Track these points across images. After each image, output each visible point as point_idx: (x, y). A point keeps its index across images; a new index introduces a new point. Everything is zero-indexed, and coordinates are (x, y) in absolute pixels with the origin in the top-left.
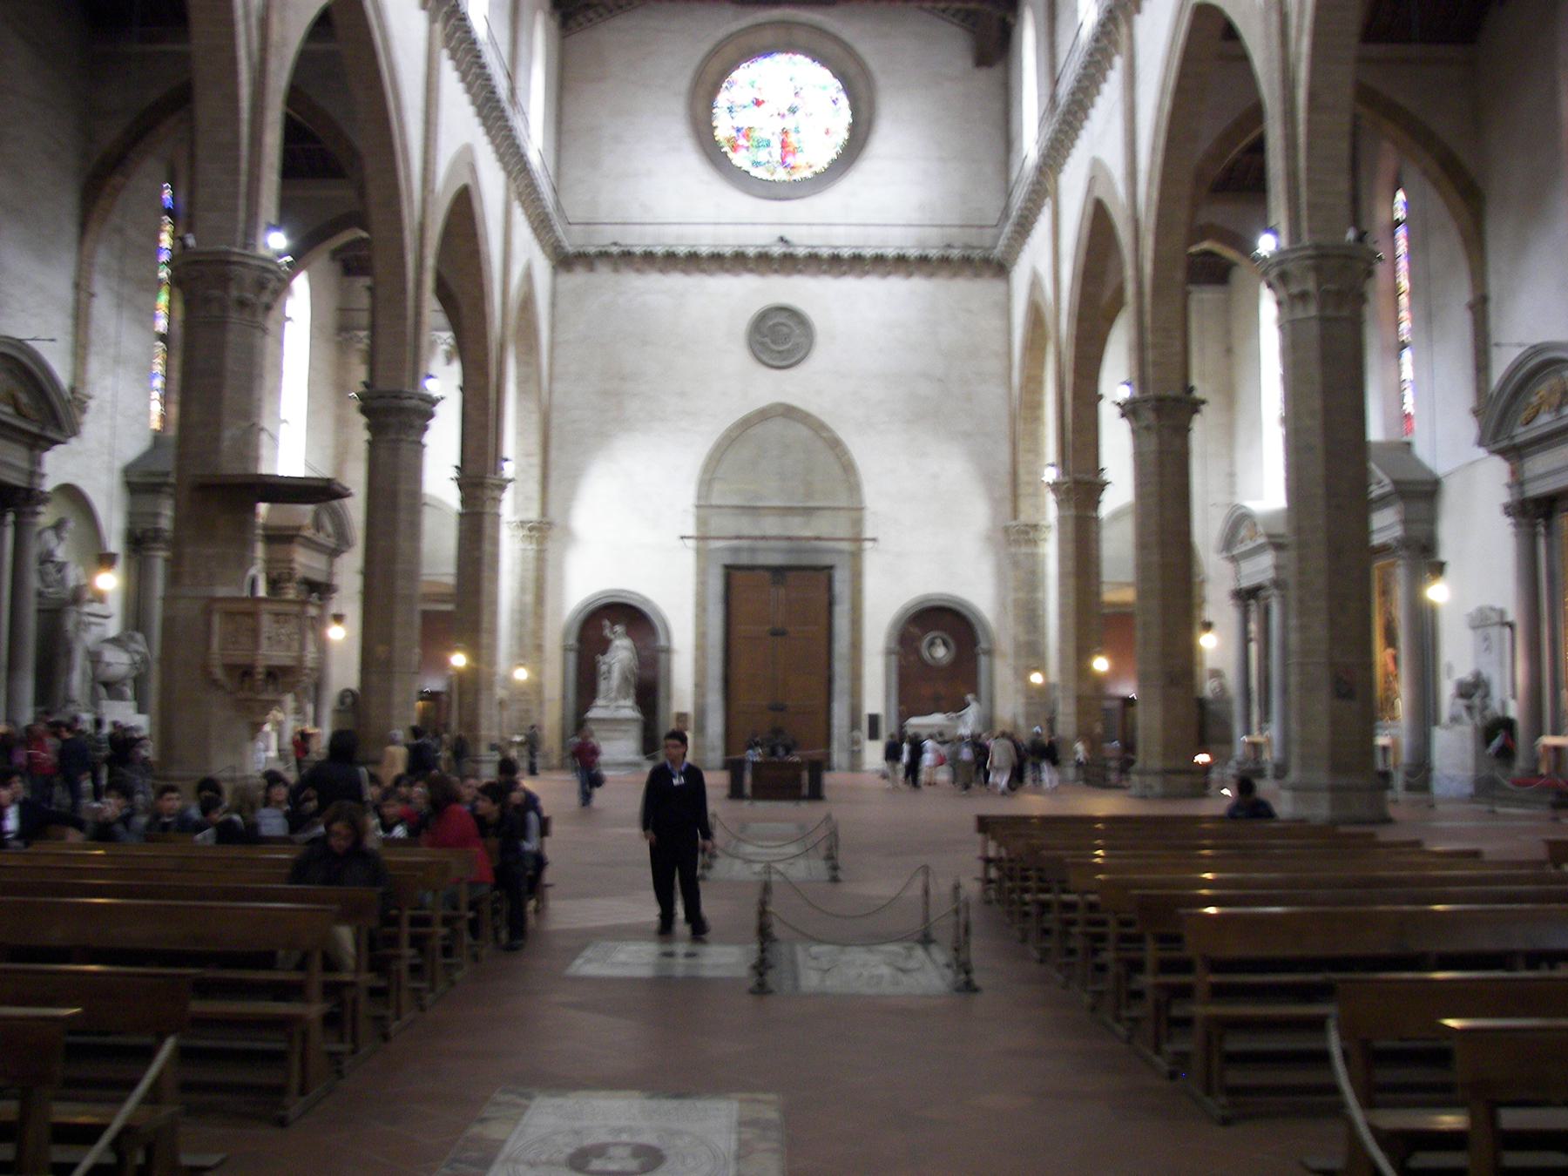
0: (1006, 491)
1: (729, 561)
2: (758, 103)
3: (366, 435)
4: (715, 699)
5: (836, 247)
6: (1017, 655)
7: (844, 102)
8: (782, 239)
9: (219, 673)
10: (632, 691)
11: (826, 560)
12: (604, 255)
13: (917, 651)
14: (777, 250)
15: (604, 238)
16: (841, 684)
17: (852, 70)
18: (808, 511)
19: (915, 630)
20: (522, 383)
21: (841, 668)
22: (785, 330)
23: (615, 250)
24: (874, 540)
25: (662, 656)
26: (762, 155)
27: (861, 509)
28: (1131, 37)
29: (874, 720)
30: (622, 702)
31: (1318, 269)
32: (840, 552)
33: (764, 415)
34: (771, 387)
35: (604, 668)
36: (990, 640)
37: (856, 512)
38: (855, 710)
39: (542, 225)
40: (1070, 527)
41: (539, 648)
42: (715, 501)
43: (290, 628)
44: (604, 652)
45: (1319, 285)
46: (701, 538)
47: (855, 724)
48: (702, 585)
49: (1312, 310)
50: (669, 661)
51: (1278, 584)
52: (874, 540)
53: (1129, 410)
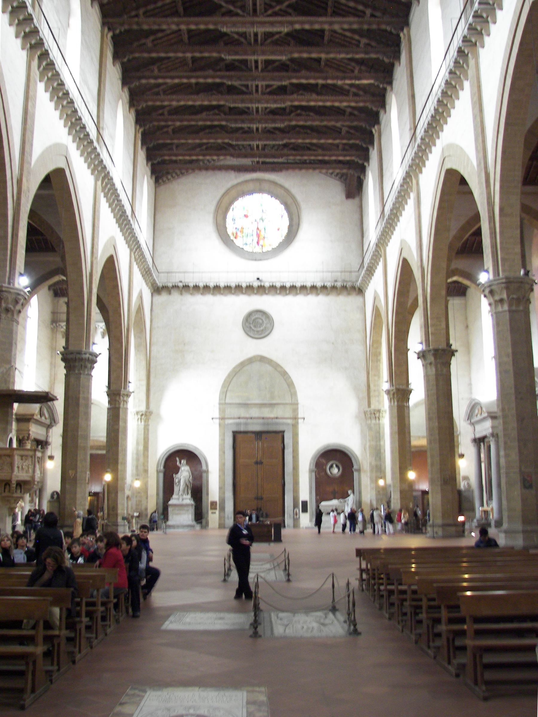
1: (235, 429)
3: (65, 371)
6: (371, 471)
7: (286, 215)
8: (258, 279)
10: (190, 492)
11: (281, 428)
12: (175, 287)
14: (256, 284)
15: (175, 279)
17: (290, 201)
18: (272, 405)
19: (324, 461)
20: (137, 347)
22: (260, 321)
23: (180, 285)
25: (204, 475)
27: (297, 404)
28: (418, 184)
29: (305, 504)
30: (184, 496)
31: (507, 288)
32: (288, 424)
33: (251, 361)
35: (176, 481)
37: (295, 406)
39: (146, 273)
40: (395, 411)
41: (146, 471)
42: (228, 401)
43: (29, 462)
44: (177, 472)
45: (508, 296)
46: (222, 418)
47: (295, 506)
49: (506, 307)
51: (492, 435)
53: (422, 355)
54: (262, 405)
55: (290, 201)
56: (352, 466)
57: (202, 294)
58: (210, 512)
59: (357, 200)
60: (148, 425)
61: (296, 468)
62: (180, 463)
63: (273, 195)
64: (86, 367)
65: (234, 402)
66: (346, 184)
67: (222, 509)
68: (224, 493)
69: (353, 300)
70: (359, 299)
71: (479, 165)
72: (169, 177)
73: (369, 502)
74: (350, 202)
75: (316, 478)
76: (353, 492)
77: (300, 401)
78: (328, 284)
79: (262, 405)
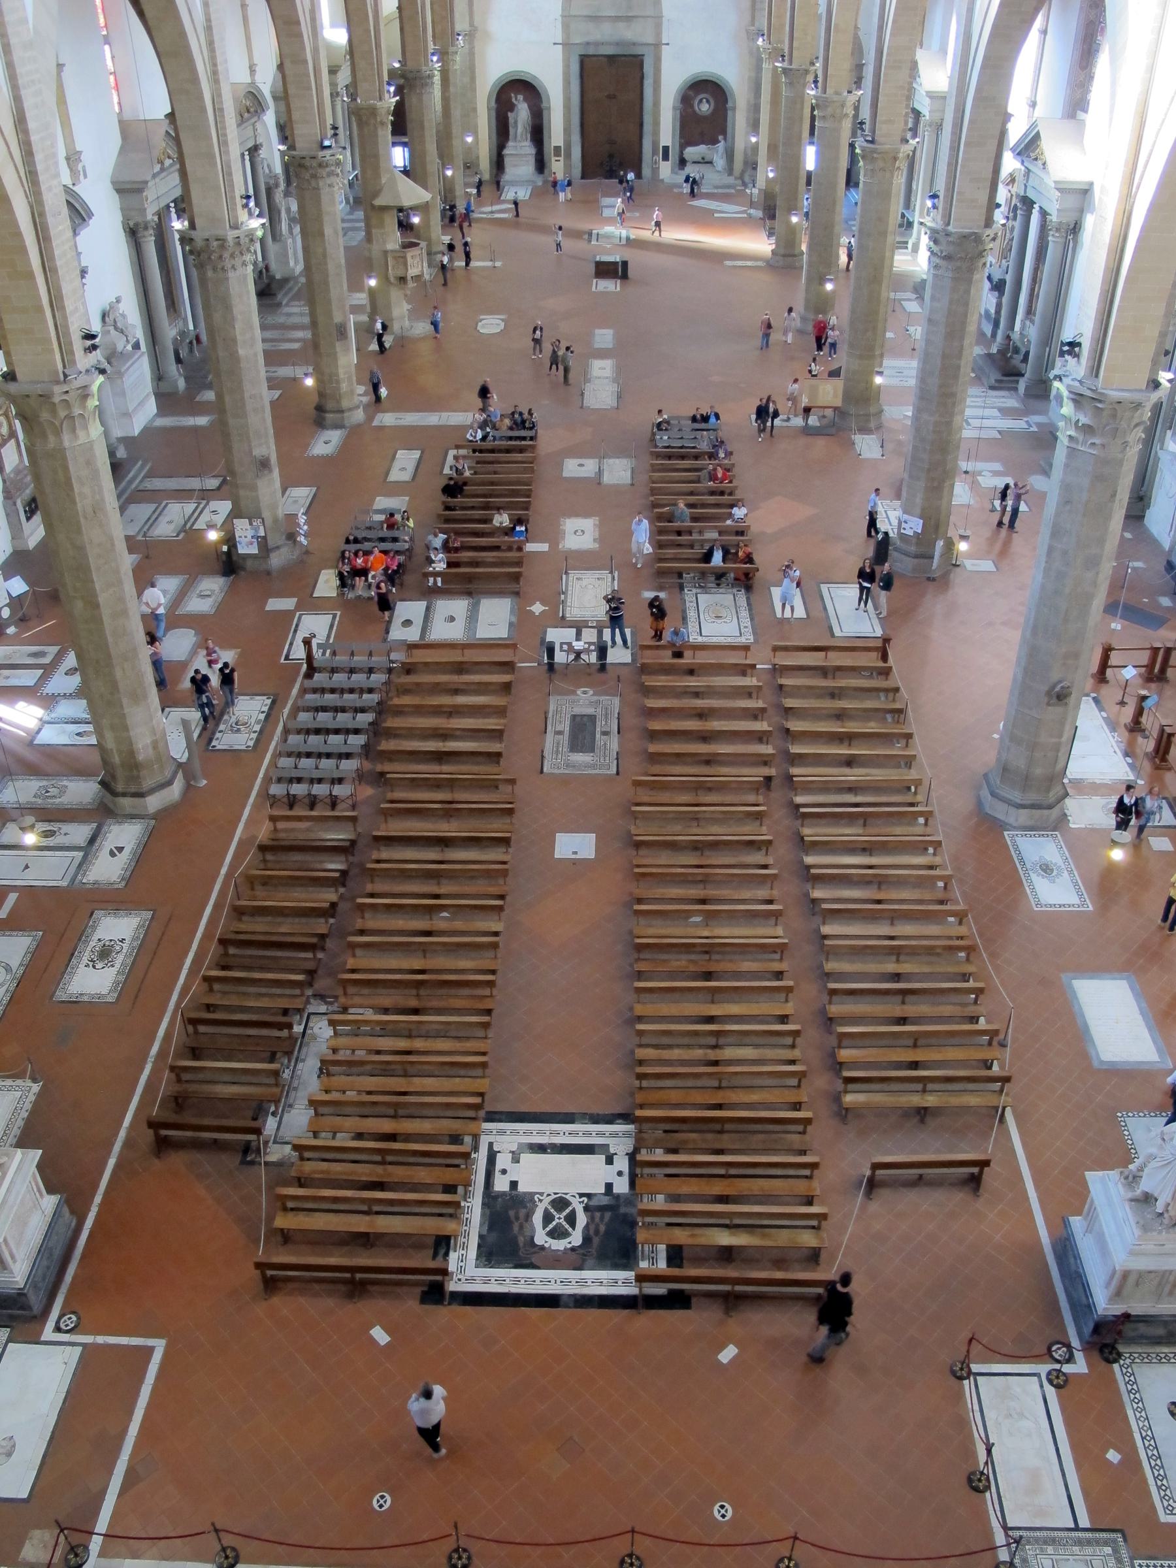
9: (392, 279)
13: (692, 106)
16: (648, 128)
18: (629, 19)
24: (668, 44)
27: (662, 17)
29: (666, 149)
35: (511, 121)
36: (735, 102)
37: (658, 20)
38: (655, 144)
42: (573, 13)
46: (566, 45)
47: (655, 152)
48: (567, 67)
52: (668, 44)
54: (617, 19)
58: (553, 159)
60: (474, 47)
61: (657, 104)
62: (516, 99)
64: (427, 85)
67: (568, 156)
75: (681, 116)
76: (725, 139)
77: (665, 13)
79: (617, 19)
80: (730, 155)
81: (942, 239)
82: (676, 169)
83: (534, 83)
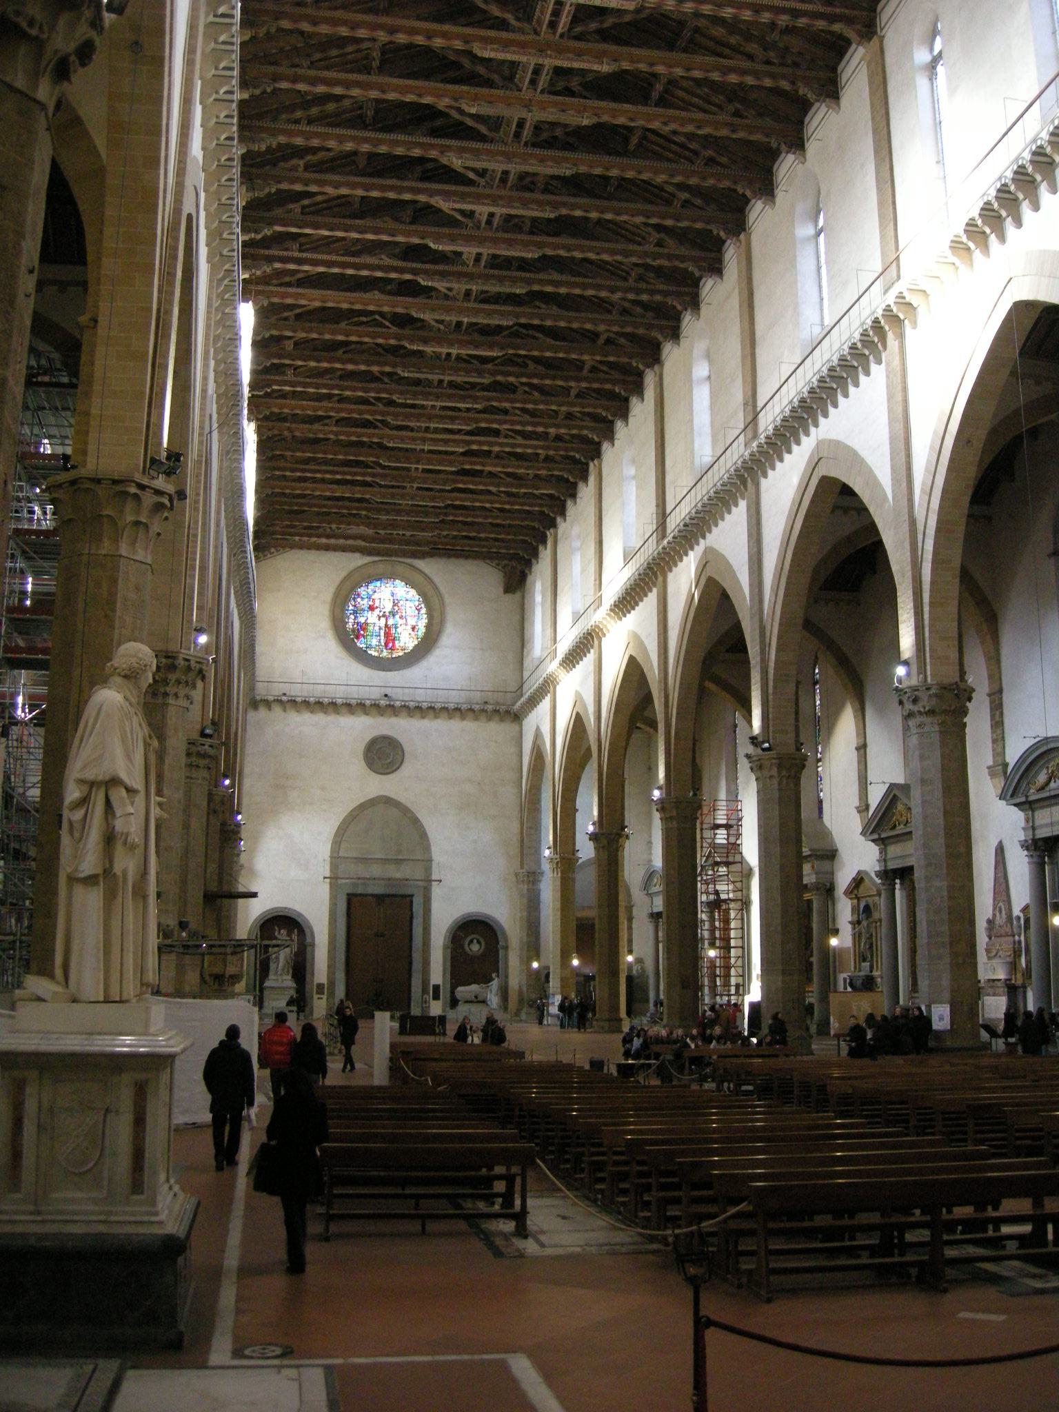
0: (515, 850)
2: (371, 608)
4: (341, 976)
5: (419, 702)
6: (521, 949)
7: (424, 611)
8: (386, 695)
9: (207, 978)
11: (408, 892)
13: (462, 947)
15: (277, 690)
16: (417, 966)
17: (431, 592)
18: (399, 862)
21: (417, 957)
23: (284, 698)
25: (309, 949)
26: (374, 642)
27: (431, 861)
29: (436, 988)
34: (377, 785)
36: (506, 941)
37: (428, 862)
38: (425, 982)
42: (342, 854)
47: (425, 991)
50: (313, 951)
55: (431, 592)
56: (497, 942)
57: (312, 712)
58: (316, 996)
59: (518, 595)
63: (409, 583)
65: (350, 856)
66: (505, 573)
67: (332, 994)
68: (334, 974)
69: (508, 728)
70: (515, 727)
71: (660, 682)
72: (273, 550)
73: (517, 987)
74: (509, 597)
78: (477, 707)
79: (386, 861)
80: (504, 993)
81: (924, 696)
82: (448, 1009)
83: (299, 920)
